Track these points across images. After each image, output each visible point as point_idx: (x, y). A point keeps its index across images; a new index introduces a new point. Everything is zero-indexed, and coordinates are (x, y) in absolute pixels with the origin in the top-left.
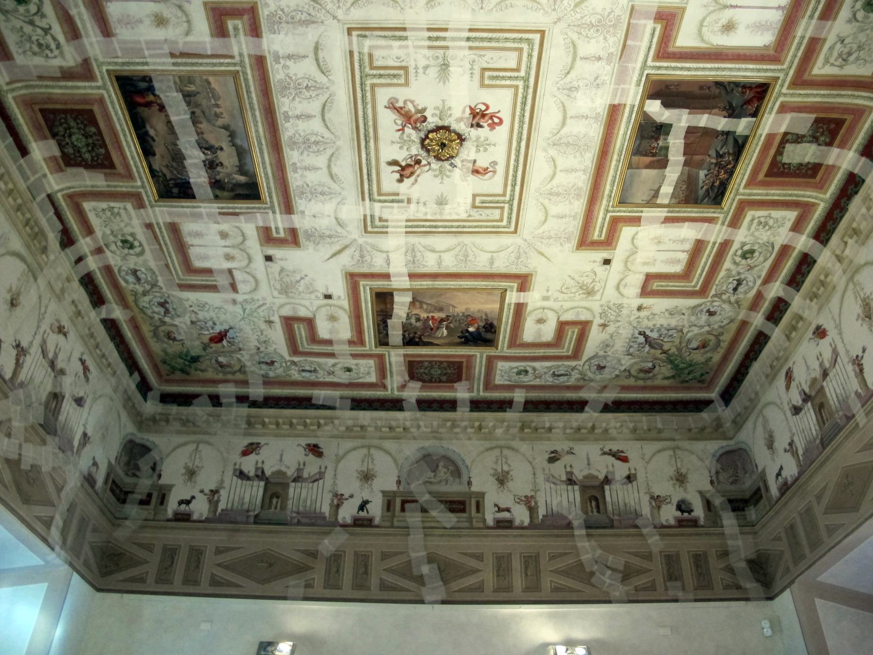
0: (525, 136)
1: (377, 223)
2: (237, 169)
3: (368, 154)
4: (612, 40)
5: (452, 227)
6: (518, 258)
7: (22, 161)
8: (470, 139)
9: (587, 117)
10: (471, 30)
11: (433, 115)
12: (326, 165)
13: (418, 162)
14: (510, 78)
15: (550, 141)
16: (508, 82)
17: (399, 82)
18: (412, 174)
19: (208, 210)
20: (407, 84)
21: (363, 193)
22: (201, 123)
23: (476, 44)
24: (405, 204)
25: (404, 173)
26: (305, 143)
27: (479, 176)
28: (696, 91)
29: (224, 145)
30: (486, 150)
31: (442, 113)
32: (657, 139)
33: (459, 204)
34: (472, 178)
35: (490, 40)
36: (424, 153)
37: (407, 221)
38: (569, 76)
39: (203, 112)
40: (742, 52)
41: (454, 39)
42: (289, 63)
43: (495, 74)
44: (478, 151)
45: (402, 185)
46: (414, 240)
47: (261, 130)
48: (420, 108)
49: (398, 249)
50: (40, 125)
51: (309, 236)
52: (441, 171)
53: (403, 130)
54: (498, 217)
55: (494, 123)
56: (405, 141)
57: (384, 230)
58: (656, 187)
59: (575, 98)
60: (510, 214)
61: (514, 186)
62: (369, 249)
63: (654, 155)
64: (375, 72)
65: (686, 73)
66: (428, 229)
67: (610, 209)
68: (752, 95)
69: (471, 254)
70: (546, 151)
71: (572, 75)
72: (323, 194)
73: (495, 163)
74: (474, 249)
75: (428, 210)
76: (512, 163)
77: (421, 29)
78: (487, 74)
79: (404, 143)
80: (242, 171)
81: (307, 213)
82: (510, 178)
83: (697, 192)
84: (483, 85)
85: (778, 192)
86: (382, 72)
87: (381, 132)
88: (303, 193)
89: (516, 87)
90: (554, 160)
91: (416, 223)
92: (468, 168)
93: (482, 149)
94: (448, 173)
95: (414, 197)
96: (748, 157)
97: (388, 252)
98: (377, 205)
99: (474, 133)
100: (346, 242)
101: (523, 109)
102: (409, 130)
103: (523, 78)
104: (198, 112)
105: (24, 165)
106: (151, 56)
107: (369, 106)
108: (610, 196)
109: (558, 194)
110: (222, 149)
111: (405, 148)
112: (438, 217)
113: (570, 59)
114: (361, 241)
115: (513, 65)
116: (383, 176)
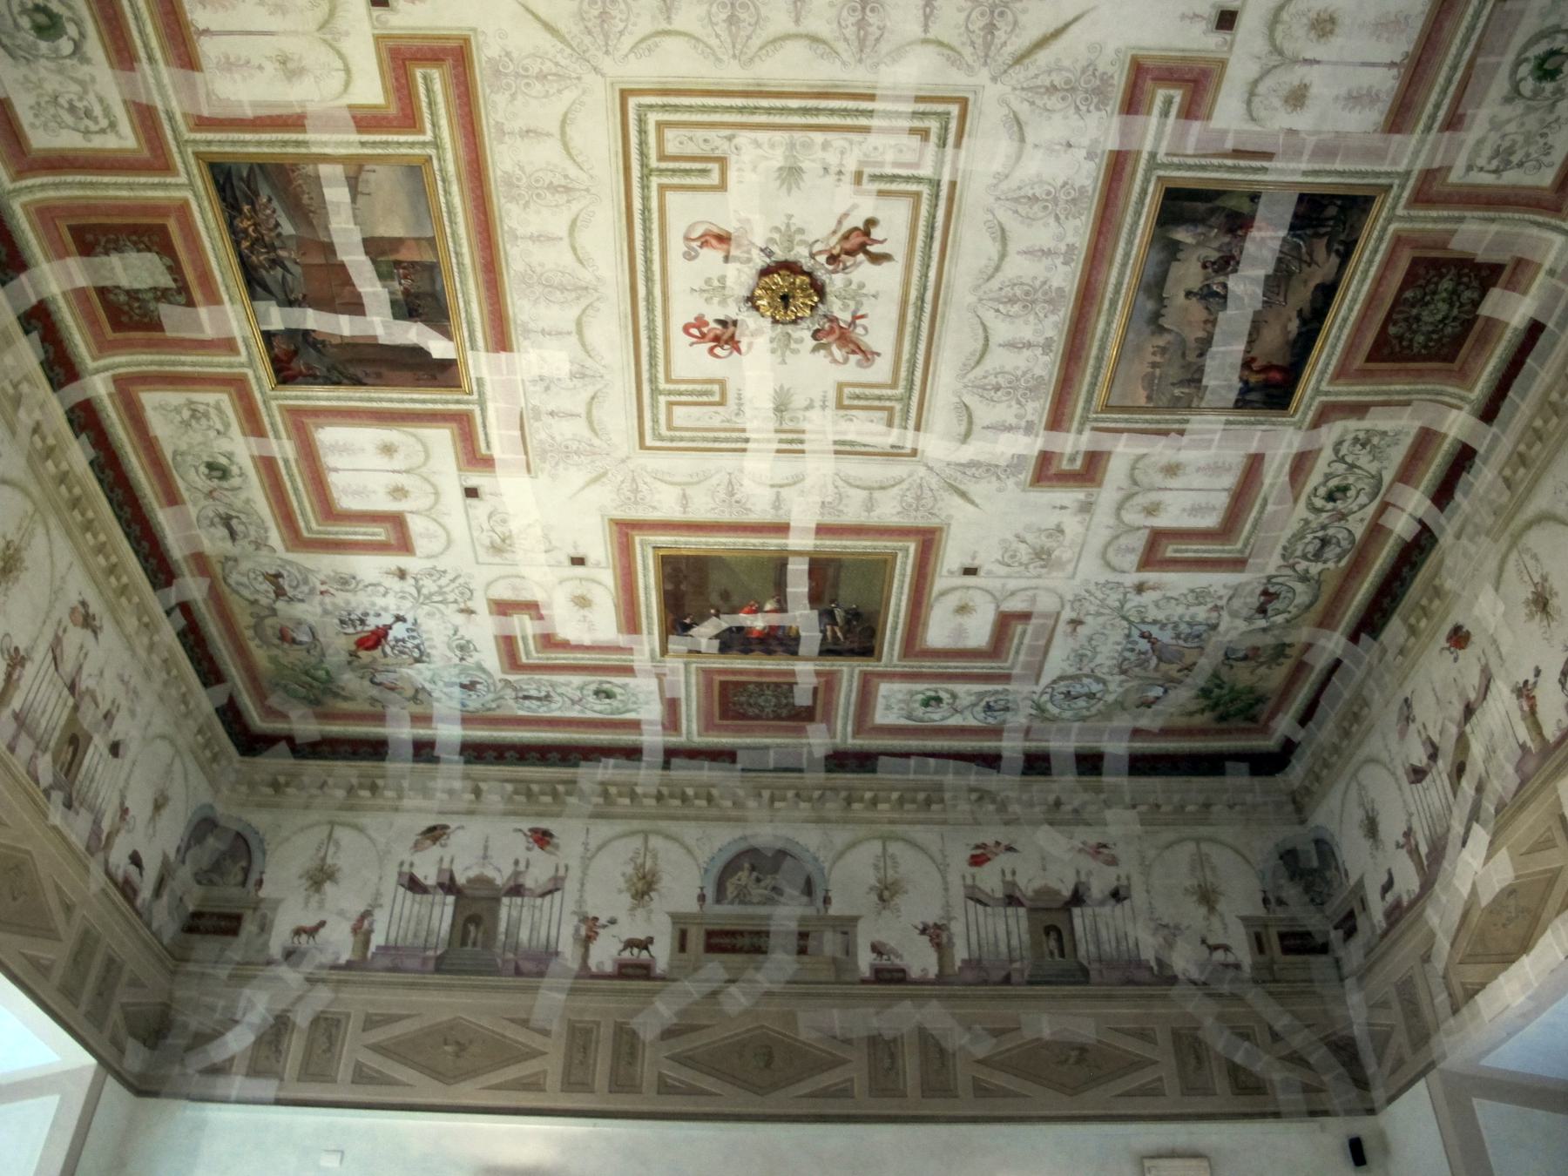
0: (642, 305)
1: (934, 125)
2: (1180, 255)
3: (925, 276)
4: (543, 436)
5: (769, 111)
6: (604, 16)
7: (1550, 325)
8: (737, 301)
9: (543, 332)
10: (744, 450)
11: (801, 341)
12: (1008, 259)
13: (833, 259)
14: (681, 393)
15: (596, 295)
16: (683, 387)
17: (852, 390)
18: (846, 237)
19: (1292, 165)
20: (840, 386)
21: (951, 199)
22: (1197, 340)
23: (735, 435)
24: (868, 171)
25: (862, 239)
26: (1033, 302)
27: (716, 230)
28: (384, 371)
29: (1180, 299)
30: (708, 281)
31: (784, 346)
32: (406, 292)
33: (754, 169)
34: (729, 225)
35: (716, 440)
36: (821, 274)
37: (866, 130)
38: (591, 394)
39: (1184, 355)
40: (349, 420)
41: (769, 441)
42: (1012, 421)
43: (705, 399)
44: (722, 279)
45: (869, 215)
46: (857, 76)
47: (1101, 325)
48: (822, 352)
49: (898, 53)
50: (1477, 340)
51: (1099, 93)
52: (790, 241)
53: (855, 318)
54: (669, 134)
55: (698, 328)
56: (853, 298)
57: (922, 107)
58: (361, 200)
59: (572, 362)
60: (642, 143)
61: (646, 209)
62: (967, 52)
63: (397, 264)
64: (888, 404)
65: (415, 396)
66: (823, 104)
67: (431, 151)
68: (293, 365)
69: (722, 29)
70: (598, 279)
71: (585, 395)
72: (1033, 199)
73: (690, 256)
74: (714, 42)
75: (820, 154)
76: (656, 257)
77: (815, 452)
78: (717, 398)
79: (855, 295)
80: (1172, 250)
81: (1083, 153)
82: (655, 226)
83: (273, 186)
84: (722, 383)
85: (112, 193)
86: (876, 403)
87: (894, 314)
88: (1074, 201)
89: (668, 380)
90: (580, 261)
91: (849, 121)
92: (739, 246)
93: (716, 283)
94: (776, 236)
95: (847, 186)
96: (226, 262)
97: (926, 41)
98: (926, 171)
99: (731, 312)
100: (1019, 75)
101: (652, 349)
102: (845, 317)
103: (661, 393)
104: (1192, 357)
105: (1555, 318)
106: (1214, 432)
107: (905, 356)
108: (444, 180)
109: (553, 188)
110: (1189, 294)
111: (854, 286)
112: (798, 136)
113: (594, 412)
114: (983, 76)
115: (677, 410)
116: (903, 233)
